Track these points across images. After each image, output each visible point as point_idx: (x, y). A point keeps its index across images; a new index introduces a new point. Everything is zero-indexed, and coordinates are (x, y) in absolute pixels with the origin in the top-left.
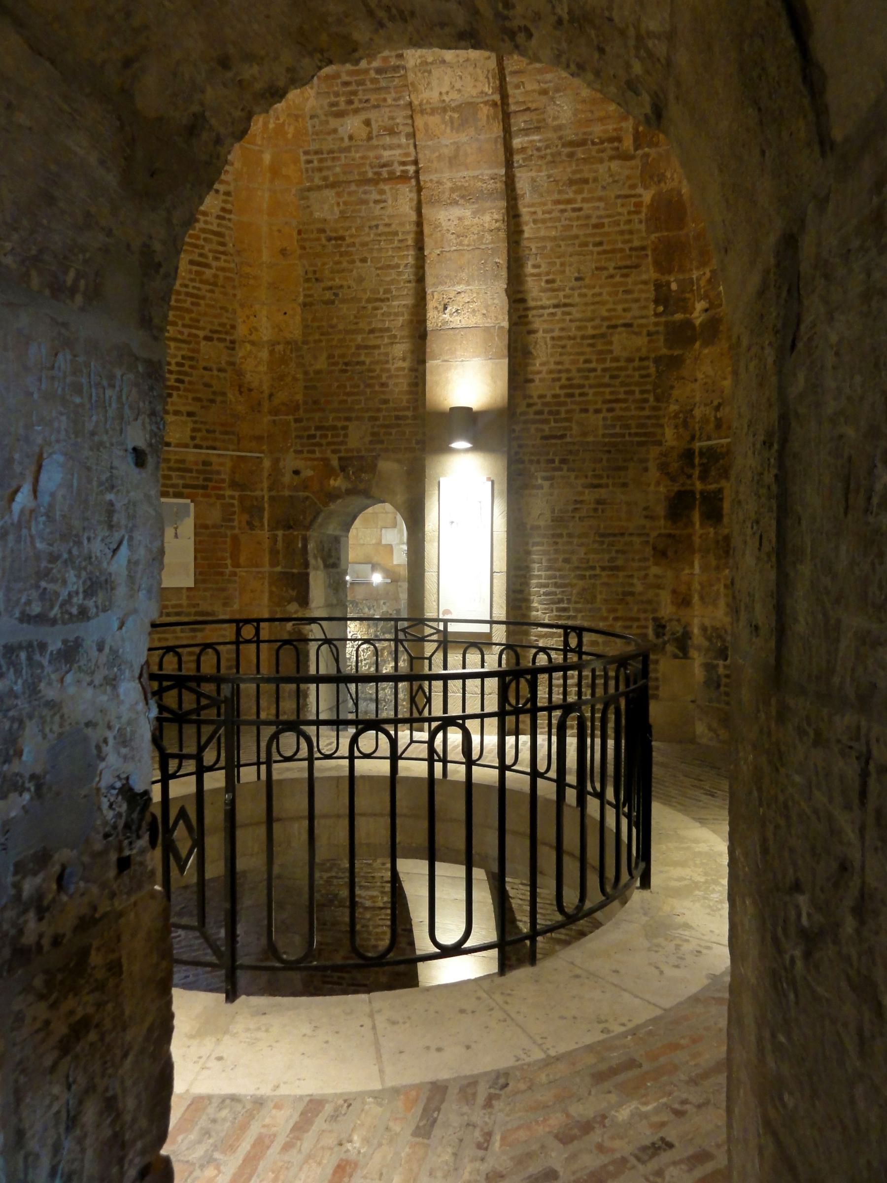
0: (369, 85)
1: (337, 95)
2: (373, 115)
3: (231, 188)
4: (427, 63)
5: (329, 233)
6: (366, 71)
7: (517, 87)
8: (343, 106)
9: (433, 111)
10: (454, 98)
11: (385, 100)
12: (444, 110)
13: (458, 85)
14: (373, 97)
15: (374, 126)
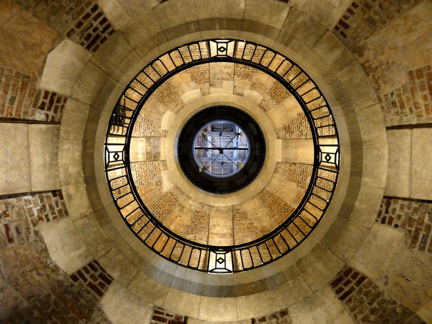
0: (198, 230)
1: (189, 230)
2: (197, 235)
3: (152, 239)
4: (215, 225)
5: (176, 256)
6: (198, 227)
7: (237, 235)
8: (190, 232)
9: (215, 234)
10: (221, 232)
11: (201, 233)
12: (218, 234)
13: (222, 230)
14: (198, 232)
15: (197, 238)
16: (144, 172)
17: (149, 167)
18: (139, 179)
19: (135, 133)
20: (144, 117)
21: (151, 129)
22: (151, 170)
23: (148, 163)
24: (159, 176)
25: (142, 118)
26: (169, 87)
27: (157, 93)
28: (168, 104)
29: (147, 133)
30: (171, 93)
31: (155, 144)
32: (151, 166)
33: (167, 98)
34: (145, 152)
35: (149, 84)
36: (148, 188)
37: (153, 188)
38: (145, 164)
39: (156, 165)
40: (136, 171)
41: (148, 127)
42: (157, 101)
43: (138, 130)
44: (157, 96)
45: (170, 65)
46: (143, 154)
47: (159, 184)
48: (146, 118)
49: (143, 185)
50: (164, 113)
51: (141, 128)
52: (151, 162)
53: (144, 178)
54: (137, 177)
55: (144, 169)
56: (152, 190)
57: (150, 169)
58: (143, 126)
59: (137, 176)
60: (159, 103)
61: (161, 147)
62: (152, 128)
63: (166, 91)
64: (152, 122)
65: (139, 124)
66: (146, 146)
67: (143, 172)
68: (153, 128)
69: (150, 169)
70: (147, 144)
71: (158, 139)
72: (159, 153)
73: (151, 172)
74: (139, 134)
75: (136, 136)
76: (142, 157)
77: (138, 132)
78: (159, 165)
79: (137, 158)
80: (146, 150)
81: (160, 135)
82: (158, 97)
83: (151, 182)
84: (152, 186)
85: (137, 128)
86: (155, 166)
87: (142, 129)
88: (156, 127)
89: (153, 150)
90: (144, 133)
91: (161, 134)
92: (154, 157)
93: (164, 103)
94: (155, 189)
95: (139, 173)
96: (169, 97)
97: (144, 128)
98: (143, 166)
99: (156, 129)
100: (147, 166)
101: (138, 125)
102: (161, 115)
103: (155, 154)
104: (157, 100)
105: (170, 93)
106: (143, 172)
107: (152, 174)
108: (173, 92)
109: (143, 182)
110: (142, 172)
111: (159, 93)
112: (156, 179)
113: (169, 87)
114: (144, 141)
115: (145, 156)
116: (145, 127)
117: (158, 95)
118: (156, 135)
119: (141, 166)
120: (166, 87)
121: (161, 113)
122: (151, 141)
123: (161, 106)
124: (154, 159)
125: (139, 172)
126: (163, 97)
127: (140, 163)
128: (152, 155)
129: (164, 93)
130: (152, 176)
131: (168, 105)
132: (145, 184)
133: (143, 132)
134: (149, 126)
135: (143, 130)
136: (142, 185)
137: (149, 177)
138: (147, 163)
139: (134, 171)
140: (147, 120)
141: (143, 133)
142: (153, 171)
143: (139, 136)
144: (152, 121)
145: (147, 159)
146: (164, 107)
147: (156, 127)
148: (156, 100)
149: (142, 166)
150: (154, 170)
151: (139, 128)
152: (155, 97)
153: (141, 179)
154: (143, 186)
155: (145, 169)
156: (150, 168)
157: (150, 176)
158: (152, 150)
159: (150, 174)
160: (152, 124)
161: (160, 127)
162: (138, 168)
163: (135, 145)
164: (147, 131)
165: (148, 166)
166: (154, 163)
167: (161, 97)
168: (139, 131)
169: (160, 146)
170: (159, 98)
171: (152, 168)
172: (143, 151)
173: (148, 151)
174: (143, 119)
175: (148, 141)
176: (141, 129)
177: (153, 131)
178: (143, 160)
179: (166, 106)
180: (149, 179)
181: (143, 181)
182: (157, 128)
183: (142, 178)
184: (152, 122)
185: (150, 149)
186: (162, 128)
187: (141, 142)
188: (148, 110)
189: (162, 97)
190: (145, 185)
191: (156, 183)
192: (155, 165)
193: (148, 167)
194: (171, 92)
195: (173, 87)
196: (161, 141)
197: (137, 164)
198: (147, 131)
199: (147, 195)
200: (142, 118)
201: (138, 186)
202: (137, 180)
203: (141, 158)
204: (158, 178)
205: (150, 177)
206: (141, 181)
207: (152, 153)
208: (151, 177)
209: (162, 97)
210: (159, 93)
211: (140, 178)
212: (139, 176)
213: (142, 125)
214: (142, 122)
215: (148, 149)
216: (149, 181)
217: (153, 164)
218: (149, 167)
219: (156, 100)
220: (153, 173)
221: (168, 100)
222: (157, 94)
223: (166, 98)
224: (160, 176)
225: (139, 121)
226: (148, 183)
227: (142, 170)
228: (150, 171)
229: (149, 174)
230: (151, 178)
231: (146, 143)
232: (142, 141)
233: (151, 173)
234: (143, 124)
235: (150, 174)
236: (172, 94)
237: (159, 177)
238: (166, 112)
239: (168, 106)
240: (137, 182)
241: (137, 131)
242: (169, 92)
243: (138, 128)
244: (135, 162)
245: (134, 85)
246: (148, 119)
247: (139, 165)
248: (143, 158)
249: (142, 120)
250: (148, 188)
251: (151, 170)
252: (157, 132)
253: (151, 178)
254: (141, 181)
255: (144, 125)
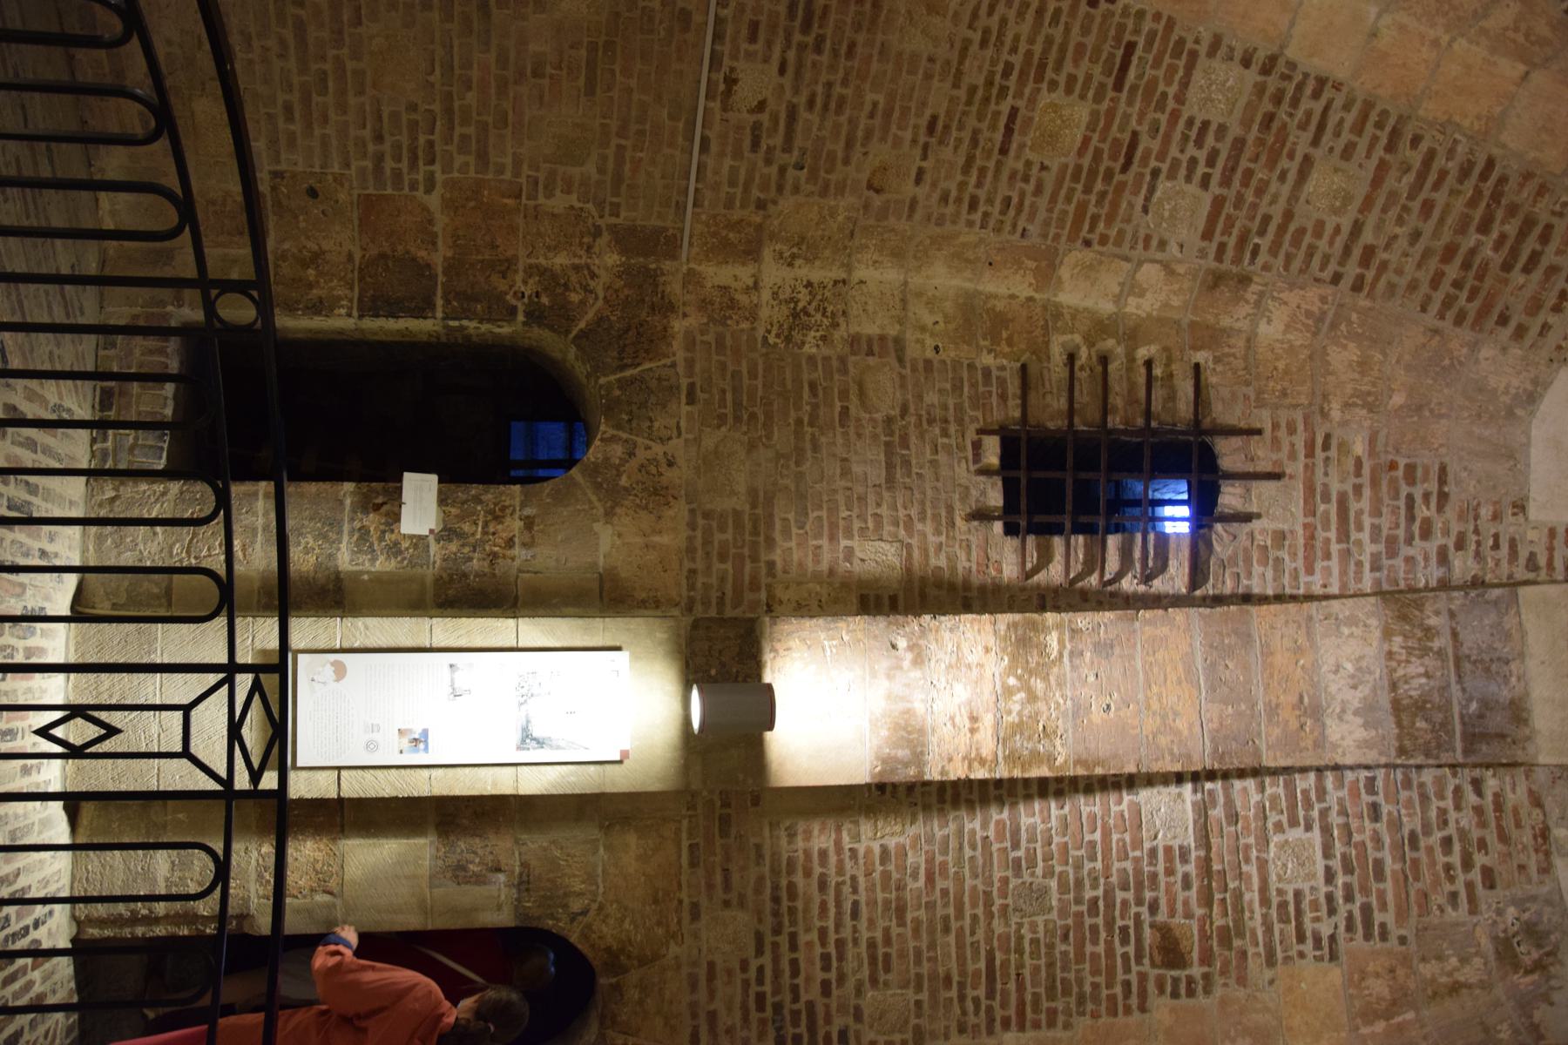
16: (1398, 847)
17: (1443, 812)
18: (1348, 888)
19: (1310, 570)
20: (1372, 453)
21: (1446, 532)
22: (1463, 834)
23: (1440, 783)
24: (1532, 889)
25: (1359, 463)
26: (1496, 196)
27: (1419, 266)
28: (1540, 319)
29: (1410, 560)
30: (1537, 230)
31: (1472, 639)
32: (1458, 808)
33: (1517, 277)
34: (1385, 700)
35: (1337, 230)
36: (1428, 970)
37: (1469, 974)
38: (1407, 784)
39: (1511, 799)
40: (1326, 830)
41: (1411, 518)
42: (1447, 325)
43: (1335, 548)
44: (1424, 288)
45: (1432, 33)
46: (1367, 711)
47: (1527, 961)
48: (1385, 459)
49: (1384, 936)
50: (1532, 399)
51: (1354, 535)
52: (1467, 774)
53: (1389, 886)
54: (1328, 869)
55: (1395, 824)
56: (1455, 988)
57: (1451, 830)
58: (1367, 521)
59: (1336, 864)
60: (1466, 333)
61: (1532, 665)
62: (1449, 522)
63: (1484, 228)
64: (1442, 481)
65: (1333, 508)
66: (1390, 655)
67: (1387, 840)
68: (1461, 517)
69: (1451, 830)
70: (1398, 640)
71: (1496, 603)
72: (1518, 712)
73: (1457, 847)
74: (1343, 573)
75: (1317, 590)
76: (1361, 734)
77: (1334, 564)
78: (1537, 802)
79: (1320, 743)
80: (1394, 686)
81: (1532, 564)
82: (1439, 297)
83: (1457, 924)
84: (1464, 960)
85: (1321, 535)
86: (1499, 805)
87: (1365, 536)
88: (1486, 512)
89: (1455, 689)
90: (1386, 562)
91: (1542, 561)
92: (1472, 739)
93: (1503, 320)
94: (1485, 986)
95: (1349, 843)
96: (1527, 270)
97: (1376, 530)
98: (1392, 798)
99: (1489, 529)
100: (1424, 798)
101: (1326, 513)
102: (1510, 413)
103: (1481, 716)
104: (1441, 316)
105: (1522, 234)
106: (1387, 840)
107: (1467, 864)
108: (1544, 218)
109: (1378, 917)
110: (1377, 840)
111: (1433, 264)
112: (1500, 912)
113: (1496, 196)
114: (1373, 622)
115: (1391, 728)
116: (1385, 522)
117: (1435, 283)
118: (1499, 566)
119: (1366, 798)
120: (1473, 203)
121: (1506, 399)
122: (1433, 621)
123: (1486, 352)
124: (1466, 752)
125: (1356, 838)
126: (1480, 277)
127: (1364, 774)
128: (1445, 725)
129: (1473, 252)
130: (1470, 886)
131: (1545, 328)
132: (1395, 931)
133: (1375, 558)
134: (1422, 512)
135: (1370, 548)
136: (1368, 936)
137: (1436, 883)
138: (1428, 776)
139: (1308, 828)
140: (1400, 472)
141: (1375, 568)
142: (1482, 845)
143: (1344, 585)
144: (1443, 470)
145: (1402, 751)
146: (1516, 351)
147: (1486, 512)
148: (1430, 318)
149: (1380, 799)
150: (1491, 837)
151: (1344, 536)
152: (1418, 297)
153: (1365, 890)
154: (1377, 944)
155: (1411, 823)
156: (1452, 815)
157: (1452, 879)
158: (1444, 688)
159: (1448, 868)
160: (1443, 497)
161: (1520, 507)
162: (1343, 812)
163: (1298, 651)
164: (1405, 551)
165: (1435, 804)
166: (1491, 783)
167: (1457, 284)
168: (1346, 555)
169: (1521, 656)
170: (1448, 303)
171: (1467, 820)
172: (1364, 691)
173: (1415, 688)
174: (1366, 470)
175: (1403, 617)
176: (1359, 543)
177: (1460, 545)
178: (1371, 757)
179: (1528, 341)
180: (1438, 899)
181: (1383, 906)
182: (1496, 517)
183: (1374, 886)
184: (1442, 481)
185: (1427, 675)
186: (1533, 512)
187: (1346, 631)
188: (1398, 399)
189: (1470, 282)
190: (1393, 942)
191: (1495, 939)
192: (1496, 795)
193: (1433, 814)
194: (1528, 224)
195: (1532, 186)
196: (1530, 619)
197: (1340, 784)
198: (1405, 551)
199: (1410, 1015)
200: (1359, 463)
201: (1332, 938)
202: (1330, 898)
203: (1349, 742)
204: (1520, 903)
205: (1448, 887)
206: (1366, 910)
207: (1446, 707)
208: (1460, 886)
209: (1470, 282)
210: (1433, 264)
211: (1354, 880)
212: (1348, 869)
213: (1360, 513)
214: (1358, 489)
215: (1407, 679)
216: (1434, 918)
217: (1479, 792)
218: (1443, 812)
219: (1430, 318)
220: (1480, 859)
221: (1528, 293)
222: (1424, 277)
223: (1506, 282)
224: (1545, 889)
225: (1335, 487)
226: (1421, 931)
227: (1382, 827)
228: (1447, 842)
229: (1441, 859)
230: (1454, 896)
231: (1387, 634)
232: (1352, 621)
233: (1456, 859)
234: (1365, 504)
235: (1448, 868)
236: (1545, 238)
237: (1534, 898)
238: (1547, 385)
239: (1553, 338)
240: (1332, 911)
241: (1328, 556)
242: (1512, 228)
243: (1333, 535)
244: (1319, 770)
245: (1234, 269)
246: (1402, 462)
247: (1355, 793)
248: (1365, 744)
249: (1358, 474)
250: (1428, 970)
251: (1463, 834)
252: (1496, 546)
253: (1454, 896)
254: (1366, 910)
255: (1376, 512)
